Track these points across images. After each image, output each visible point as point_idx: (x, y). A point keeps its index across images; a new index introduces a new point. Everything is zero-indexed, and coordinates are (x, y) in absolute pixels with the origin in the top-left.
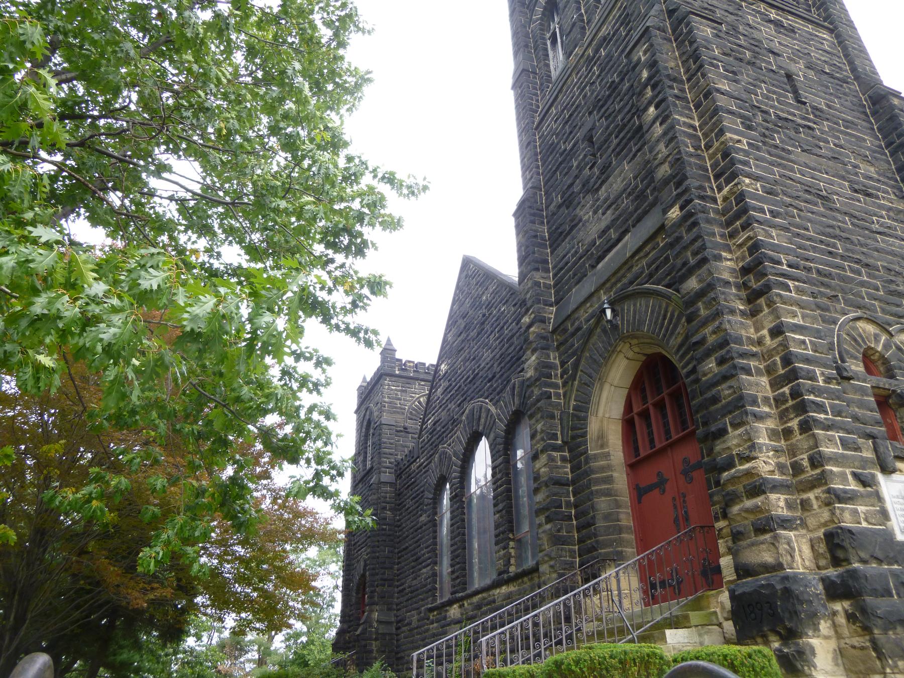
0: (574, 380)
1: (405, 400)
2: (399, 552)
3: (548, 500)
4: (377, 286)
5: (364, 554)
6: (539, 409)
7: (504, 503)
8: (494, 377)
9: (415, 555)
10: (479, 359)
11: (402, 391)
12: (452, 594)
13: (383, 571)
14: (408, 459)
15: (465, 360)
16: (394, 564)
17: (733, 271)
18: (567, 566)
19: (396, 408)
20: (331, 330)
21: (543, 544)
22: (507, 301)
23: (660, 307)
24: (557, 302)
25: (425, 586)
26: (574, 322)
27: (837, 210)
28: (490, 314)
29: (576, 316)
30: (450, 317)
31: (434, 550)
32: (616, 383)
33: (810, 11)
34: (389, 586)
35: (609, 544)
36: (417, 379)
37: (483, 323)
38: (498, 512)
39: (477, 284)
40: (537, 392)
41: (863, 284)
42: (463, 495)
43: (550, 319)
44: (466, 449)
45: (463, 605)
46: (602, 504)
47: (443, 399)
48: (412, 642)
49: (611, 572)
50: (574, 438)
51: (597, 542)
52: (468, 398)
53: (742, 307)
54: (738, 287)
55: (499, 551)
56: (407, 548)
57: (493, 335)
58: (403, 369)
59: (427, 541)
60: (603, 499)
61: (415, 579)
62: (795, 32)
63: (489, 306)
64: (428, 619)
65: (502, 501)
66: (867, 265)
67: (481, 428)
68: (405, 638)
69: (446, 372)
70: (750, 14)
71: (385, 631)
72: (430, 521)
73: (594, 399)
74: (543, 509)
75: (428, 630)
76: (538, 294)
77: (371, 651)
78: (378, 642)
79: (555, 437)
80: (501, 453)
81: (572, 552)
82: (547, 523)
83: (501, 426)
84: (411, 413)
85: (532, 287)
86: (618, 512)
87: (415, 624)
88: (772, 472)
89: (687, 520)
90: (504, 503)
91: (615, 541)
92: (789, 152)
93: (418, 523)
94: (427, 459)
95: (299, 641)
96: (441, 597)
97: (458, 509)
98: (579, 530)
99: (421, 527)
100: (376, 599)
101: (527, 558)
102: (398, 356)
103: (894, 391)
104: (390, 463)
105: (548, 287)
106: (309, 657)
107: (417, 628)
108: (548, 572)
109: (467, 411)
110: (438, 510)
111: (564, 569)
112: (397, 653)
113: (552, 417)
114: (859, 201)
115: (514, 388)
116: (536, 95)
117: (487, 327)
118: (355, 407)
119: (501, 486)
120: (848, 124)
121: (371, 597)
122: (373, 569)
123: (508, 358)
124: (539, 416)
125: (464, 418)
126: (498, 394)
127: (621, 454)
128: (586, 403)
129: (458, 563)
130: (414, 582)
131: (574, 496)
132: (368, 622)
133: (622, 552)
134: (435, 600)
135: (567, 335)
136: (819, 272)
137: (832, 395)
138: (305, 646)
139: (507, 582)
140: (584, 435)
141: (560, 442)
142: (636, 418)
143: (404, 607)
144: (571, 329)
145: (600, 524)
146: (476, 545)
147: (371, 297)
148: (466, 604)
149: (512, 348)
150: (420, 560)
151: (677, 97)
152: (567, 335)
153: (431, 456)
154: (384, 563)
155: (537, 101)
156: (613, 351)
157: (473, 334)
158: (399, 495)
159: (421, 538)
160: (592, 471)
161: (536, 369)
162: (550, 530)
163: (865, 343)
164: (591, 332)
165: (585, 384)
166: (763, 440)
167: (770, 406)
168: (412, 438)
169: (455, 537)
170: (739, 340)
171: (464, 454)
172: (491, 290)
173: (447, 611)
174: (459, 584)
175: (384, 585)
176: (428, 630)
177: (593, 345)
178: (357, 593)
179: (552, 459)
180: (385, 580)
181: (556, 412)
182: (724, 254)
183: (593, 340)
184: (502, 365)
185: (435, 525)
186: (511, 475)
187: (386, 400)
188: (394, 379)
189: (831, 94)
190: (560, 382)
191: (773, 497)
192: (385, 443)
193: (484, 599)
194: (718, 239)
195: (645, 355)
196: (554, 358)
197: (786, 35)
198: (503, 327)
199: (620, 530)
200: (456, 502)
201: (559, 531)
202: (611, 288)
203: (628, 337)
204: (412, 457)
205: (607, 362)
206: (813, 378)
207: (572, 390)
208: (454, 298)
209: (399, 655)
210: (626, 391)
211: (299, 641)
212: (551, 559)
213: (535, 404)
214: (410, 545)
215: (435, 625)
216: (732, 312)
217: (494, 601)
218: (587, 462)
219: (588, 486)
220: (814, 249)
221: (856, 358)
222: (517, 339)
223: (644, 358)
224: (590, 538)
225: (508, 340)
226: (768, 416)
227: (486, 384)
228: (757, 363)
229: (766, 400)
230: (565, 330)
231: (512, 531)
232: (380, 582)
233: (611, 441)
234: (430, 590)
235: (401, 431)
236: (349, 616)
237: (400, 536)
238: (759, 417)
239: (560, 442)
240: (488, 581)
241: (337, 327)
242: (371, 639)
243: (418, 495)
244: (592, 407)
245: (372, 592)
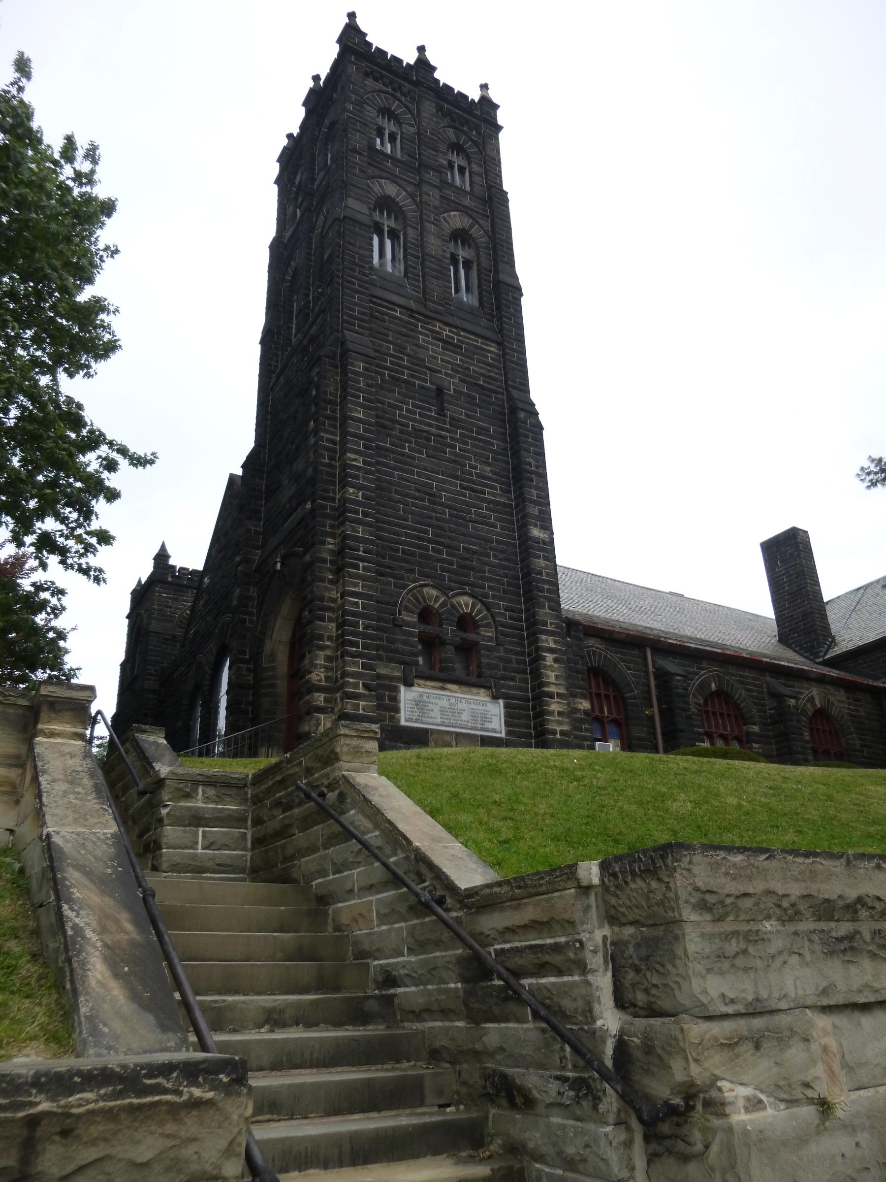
1: (175, 608)
4: (105, 538)
17: (332, 552)
20: (66, 569)
27: (441, 505)
33: (493, 321)
41: (443, 561)
43: (255, 560)
53: (330, 577)
54: (332, 563)
62: (461, 348)
66: (449, 547)
70: (422, 334)
88: (320, 681)
92: (413, 458)
102: (172, 562)
103: (438, 635)
114: (465, 496)
116: (277, 355)
118: (127, 611)
120: (482, 431)
136: (404, 552)
137: (364, 636)
141: (247, 657)
147: (97, 546)
151: (327, 417)
155: (277, 362)
163: (425, 601)
166: (320, 661)
167: (332, 641)
170: (322, 599)
182: (328, 539)
187: (156, 607)
189: (476, 405)
190: (255, 611)
191: (317, 694)
194: (328, 529)
197: (452, 352)
206: (356, 625)
216: (323, 580)
220: (407, 535)
221: (412, 612)
226: (327, 647)
228: (330, 614)
229: (330, 638)
238: (322, 648)
239: (247, 657)
241: (72, 567)
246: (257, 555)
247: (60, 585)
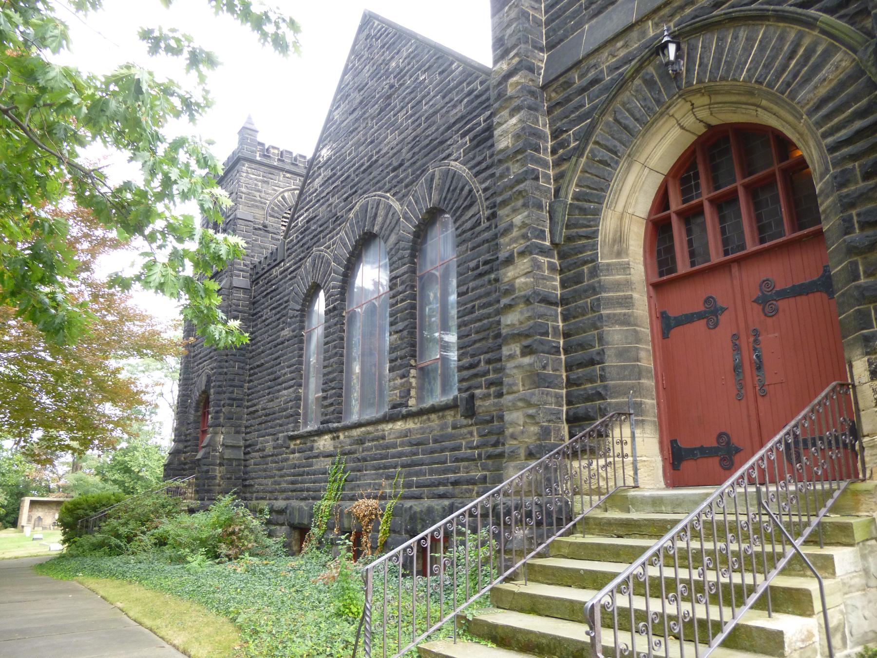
0: (581, 155)
2: (251, 369)
3: (531, 322)
5: (207, 368)
6: (520, 192)
7: (406, 323)
8: (401, 165)
9: (272, 373)
10: (380, 143)
11: (264, 182)
12: (322, 423)
13: (231, 389)
14: (268, 261)
15: (358, 145)
16: (244, 381)
18: (553, 417)
19: (255, 201)
21: (515, 384)
22: (429, 68)
23: (782, 39)
24: (550, 47)
25: (285, 410)
26: (588, 70)
28: (401, 85)
29: (592, 61)
30: (340, 90)
31: (299, 370)
32: (652, 163)
35: (618, 393)
36: (282, 170)
37: (389, 97)
38: (397, 332)
39: (382, 47)
40: (515, 169)
42: (343, 309)
43: (540, 68)
44: (352, 254)
45: (338, 437)
46: (615, 335)
47: (323, 191)
48: (265, 470)
49: (627, 431)
50: (569, 239)
51: (605, 387)
52: (360, 191)
55: (394, 380)
56: (262, 364)
57: (404, 111)
58: (264, 156)
59: (289, 359)
60: (617, 328)
61: (272, 400)
63: (400, 74)
64: (288, 448)
65: (402, 320)
67: (376, 229)
68: (255, 464)
69: (329, 159)
71: (232, 457)
72: (295, 337)
73: (614, 184)
74: (519, 335)
75: (287, 460)
76: (525, 30)
77: (214, 478)
78: (222, 468)
79: (541, 235)
80: (406, 260)
81: (558, 397)
82: (523, 354)
83: (407, 228)
84: (273, 208)
85: (517, 19)
86: (638, 348)
87: (269, 450)
89: (759, 368)
90: (406, 323)
91: (632, 388)
93: (279, 337)
94: (295, 263)
96: (305, 424)
97: (335, 325)
98: (569, 368)
99: (283, 343)
100: (222, 420)
101: (431, 392)
102: (260, 138)
104: (245, 265)
105: (538, 23)
107: (272, 455)
108: (521, 422)
109: (357, 207)
110: (306, 324)
111: (549, 421)
112: (245, 480)
113: (540, 207)
115: (432, 180)
117: (396, 102)
119: (402, 301)
121: (216, 418)
122: (220, 386)
123: (427, 141)
124: (520, 203)
125: (351, 215)
126: (406, 186)
127: (641, 268)
128: (602, 190)
129: (333, 388)
130: (271, 404)
131: (565, 320)
132: (211, 445)
133: (641, 403)
134: (296, 428)
135: (570, 91)
139: (405, 417)
140: (593, 235)
141: (547, 243)
142: (674, 219)
143: (255, 431)
144: (578, 83)
145: (611, 362)
146: (357, 369)
148: (342, 436)
149: (434, 128)
150: (280, 380)
152: (570, 91)
153: (301, 259)
154: (234, 380)
156: (662, 114)
157: (373, 110)
158: (254, 303)
159: (282, 355)
160: (603, 288)
161: (517, 136)
162: (531, 365)
164: (622, 84)
165: (600, 162)
168: (272, 238)
169: (330, 358)
171: (349, 260)
172: (405, 54)
173: (314, 441)
174: (333, 413)
175: (232, 405)
176: (287, 460)
177: (624, 104)
178: (196, 411)
179: (537, 266)
180: (234, 399)
181: (544, 201)
183: (625, 96)
184: (416, 149)
185: (301, 342)
186: (417, 289)
187: (244, 190)
188: (254, 166)
190: (550, 159)
193: (369, 433)
195: (709, 126)
196: (544, 125)
198: (420, 102)
199: (639, 373)
200: (334, 317)
201: (544, 368)
202: (672, 15)
203: (698, 91)
204: (274, 260)
205: (647, 131)
207: (574, 171)
208: (347, 66)
209: (247, 483)
210: (660, 179)
212: (529, 405)
213: (512, 187)
214: (267, 362)
215: (297, 455)
217: (383, 438)
218: (594, 272)
219: (596, 307)
222: (442, 116)
223: (702, 130)
224: (592, 380)
225: (427, 119)
227: (388, 174)
230: (568, 84)
231: (413, 356)
232: (228, 402)
233: (631, 248)
234: (292, 416)
235: (260, 229)
236: (186, 435)
237: (253, 351)
240: (372, 414)
243: (281, 304)
244: (609, 196)
245: (217, 412)
246: (542, 61)
247: (201, 43)
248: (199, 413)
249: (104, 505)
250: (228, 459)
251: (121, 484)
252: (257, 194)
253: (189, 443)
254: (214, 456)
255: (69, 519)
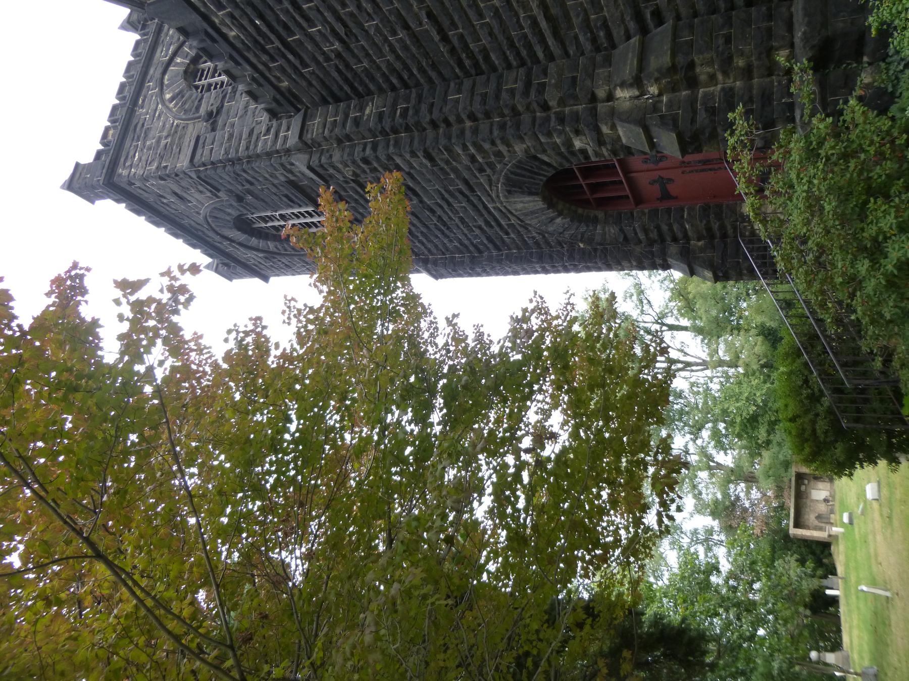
13: (504, 95)
34: (545, 74)
71: (667, 46)
95: (724, 432)
106: (744, 414)
118: (257, 281)
138: (731, 424)
175: (543, 85)
180: (528, 84)
192: (227, 153)
211: (724, 432)
236: (651, 243)
242: (693, 101)
248: (600, 214)
249: (806, 381)
250: (673, 55)
251: (772, 424)
252: (163, 142)
253: (665, 228)
254: (670, 104)
255: (839, 451)
